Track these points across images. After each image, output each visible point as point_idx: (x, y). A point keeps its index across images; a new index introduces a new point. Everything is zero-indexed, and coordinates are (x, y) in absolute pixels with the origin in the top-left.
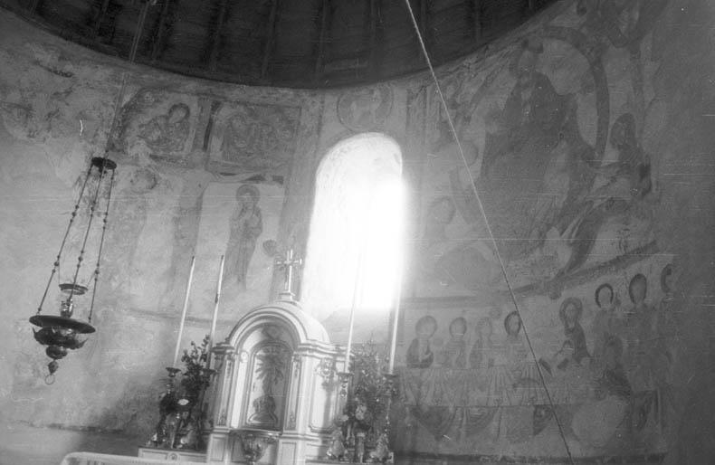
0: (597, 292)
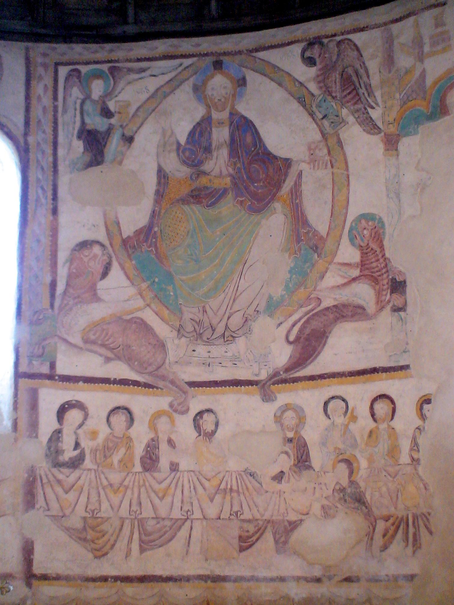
0: (326, 404)
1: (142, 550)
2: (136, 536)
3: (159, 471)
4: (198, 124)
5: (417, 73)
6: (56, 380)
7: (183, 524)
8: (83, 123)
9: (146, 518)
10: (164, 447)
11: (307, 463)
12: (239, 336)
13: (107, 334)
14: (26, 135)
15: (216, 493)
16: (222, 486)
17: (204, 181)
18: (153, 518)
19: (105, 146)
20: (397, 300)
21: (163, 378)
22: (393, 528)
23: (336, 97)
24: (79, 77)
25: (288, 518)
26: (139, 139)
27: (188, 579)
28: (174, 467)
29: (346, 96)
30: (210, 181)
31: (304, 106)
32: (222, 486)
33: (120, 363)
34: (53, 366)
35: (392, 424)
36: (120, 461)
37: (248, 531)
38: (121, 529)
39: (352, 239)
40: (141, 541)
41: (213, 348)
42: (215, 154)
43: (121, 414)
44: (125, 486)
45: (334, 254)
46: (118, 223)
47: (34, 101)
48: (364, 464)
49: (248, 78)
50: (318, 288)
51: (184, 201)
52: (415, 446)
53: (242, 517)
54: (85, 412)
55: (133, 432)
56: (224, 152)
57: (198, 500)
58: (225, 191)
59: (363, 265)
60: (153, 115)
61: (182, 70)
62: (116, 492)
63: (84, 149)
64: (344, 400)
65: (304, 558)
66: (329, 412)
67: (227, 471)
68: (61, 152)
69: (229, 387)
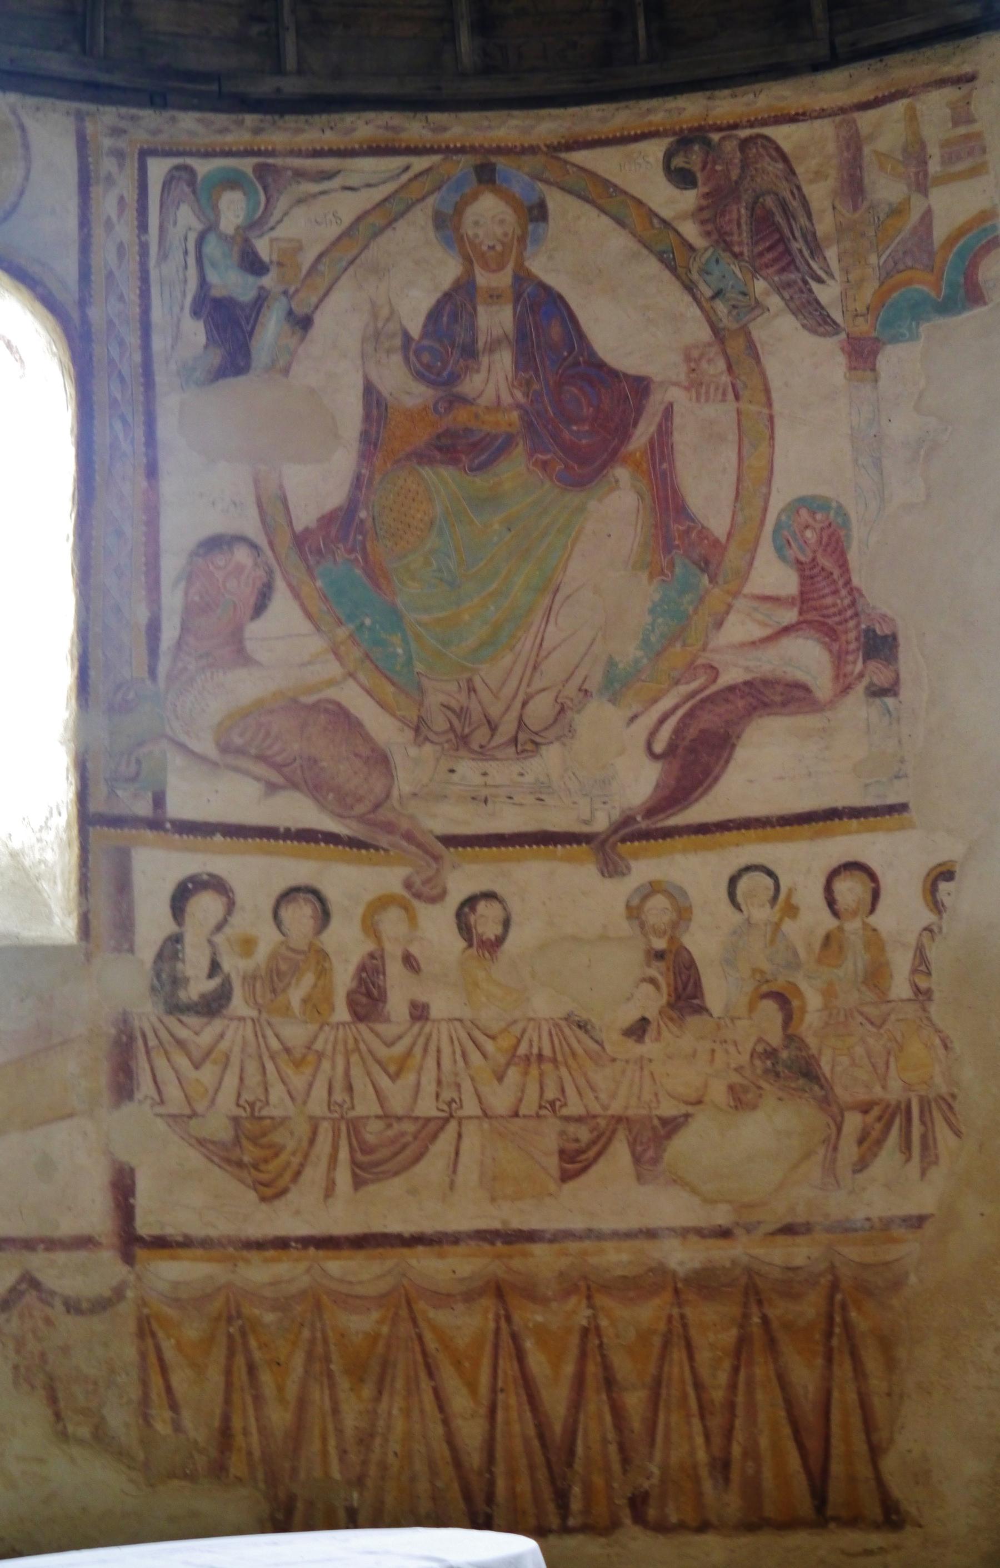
0: (733, 882)
1: (358, 1183)
2: (344, 1154)
3: (387, 1020)
4: (447, 296)
5: (915, 217)
6: (166, 831)
7: (442, 1128)
8: (203, 283)
9: (362, 1118)
10: (395, 969)
11: (696, 1001)
12: (547, 741)
13: (268, 734)
14: (83, 303)
15: (508, 1064)
16: (522, 1050)
17: (462, 416)
18: (378, 1117)
19: (251, 333)
20: (878, 674)
21: (389, 828)
22: (878, 1126)
23: (742, 254)
24: (192, 183)
25: (658, 1112)
26: (322, 321)
27: (455, 1239)
28: (419, 1012)
29: (761, 254)
30: (476, 416)
31: (673, 270)
32: (522, 1050)
33: (297, 795)
34: (159, 801)
35: (873, 920)
36: (305, 1001)
37: (577, 1140)
38: (312, 1141)
39: (780, 551)
40: (354, 1163)
41: (491, 767)
42: (485, 360)
43: (302, 902)
44: (317, 1051)
45: (744, 575)
46: (284, 501)
47: (98, 231)
48: (814, 1000)
49: (551, 205)
50: (710, 646)
51: (422, 457)
52: (921, 964)
53: (565, 1112)
54: (228, 897)
55: (332, 938)
56: (504, 360)
57: (472, 1079)
58: (509, 442)
59: (804, 599)
60: (351, 271)
61: (410, 180)
62: (298, 1064)
63: (207, 338)
64: (770, 873)
65: (694, 1191)
66: (740, 898)
67: (530, 1019)
68: (158, 343)
69: (530, 846)
